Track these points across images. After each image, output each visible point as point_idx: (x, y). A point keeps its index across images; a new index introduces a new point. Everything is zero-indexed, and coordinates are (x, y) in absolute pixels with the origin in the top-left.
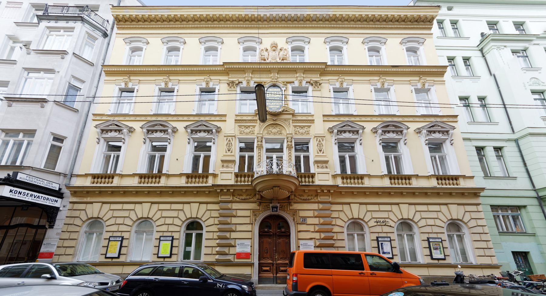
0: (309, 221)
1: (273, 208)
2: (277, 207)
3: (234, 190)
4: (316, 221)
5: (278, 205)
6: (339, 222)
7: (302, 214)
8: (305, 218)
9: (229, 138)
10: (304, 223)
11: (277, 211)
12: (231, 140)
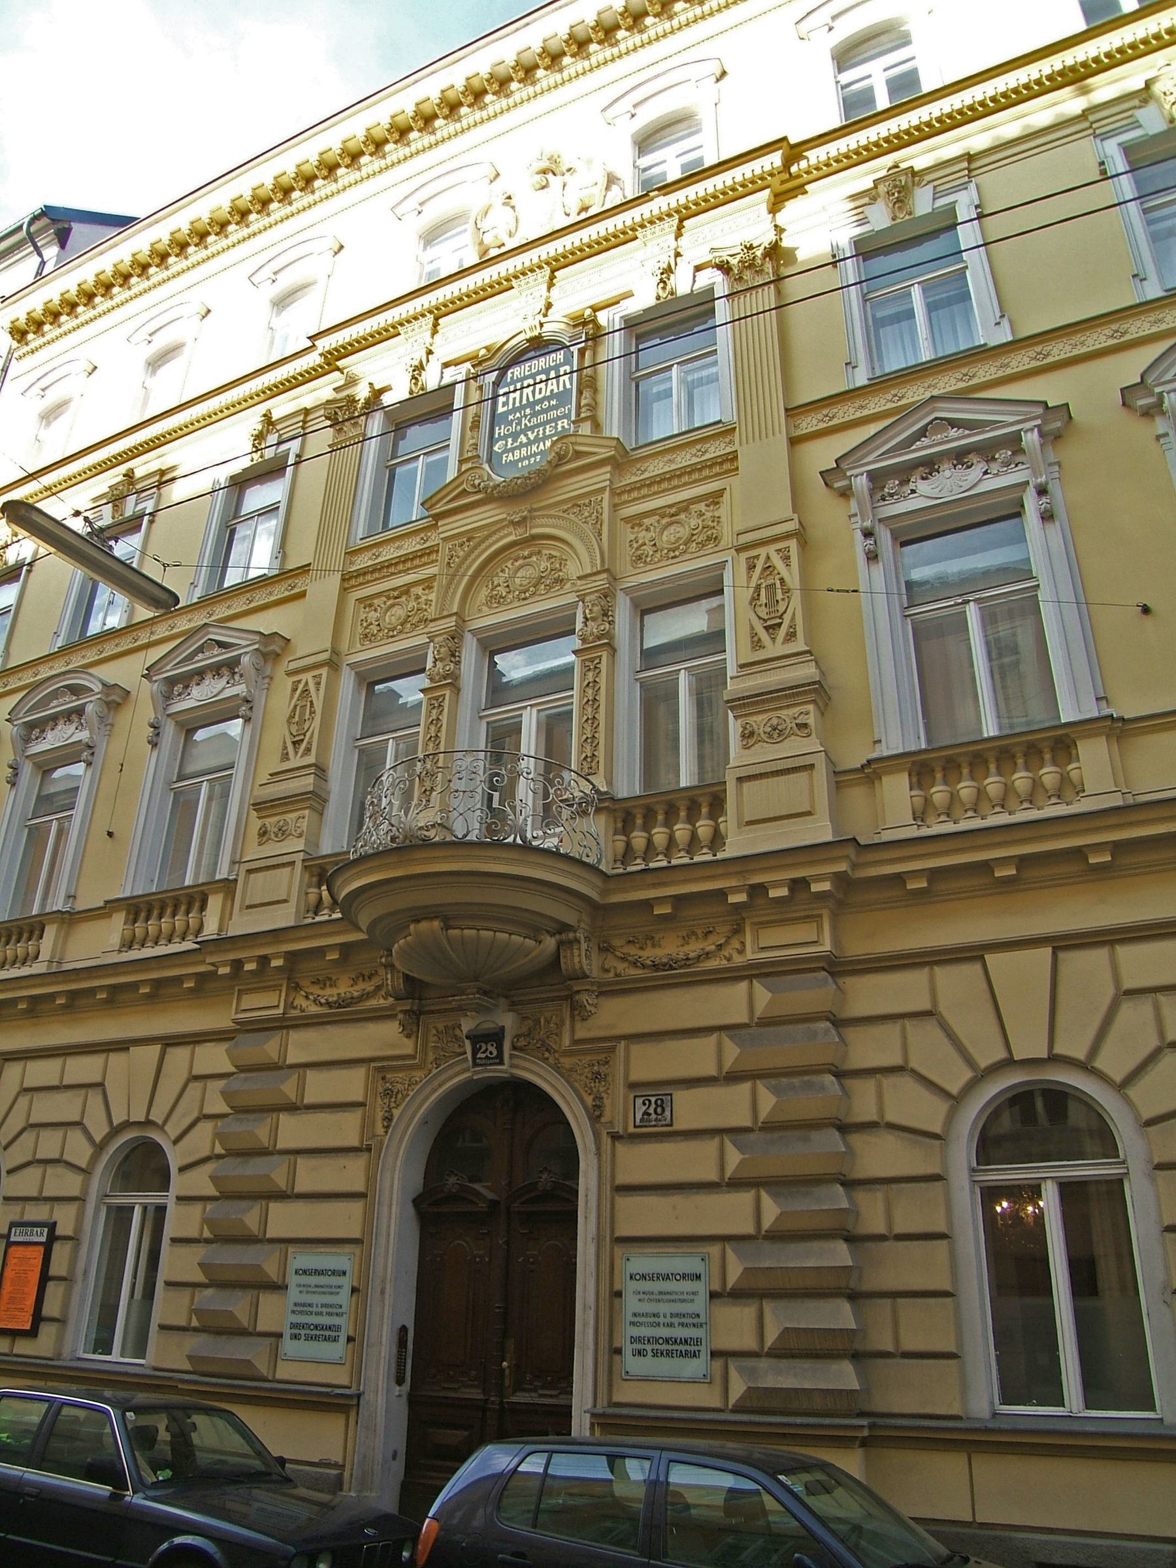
0: (689, 1109)
1: (477, 1039)
2: (496, 1037)
3: (291, 956)
4: (734, 1105)
5: (507, 1020)
6: (909, 1104)
7: (649, 1064)
8: (657, 1094)
9: (762, 551)
10: (657, 1128)
11: (500, 1060)
12: (777, 561)
